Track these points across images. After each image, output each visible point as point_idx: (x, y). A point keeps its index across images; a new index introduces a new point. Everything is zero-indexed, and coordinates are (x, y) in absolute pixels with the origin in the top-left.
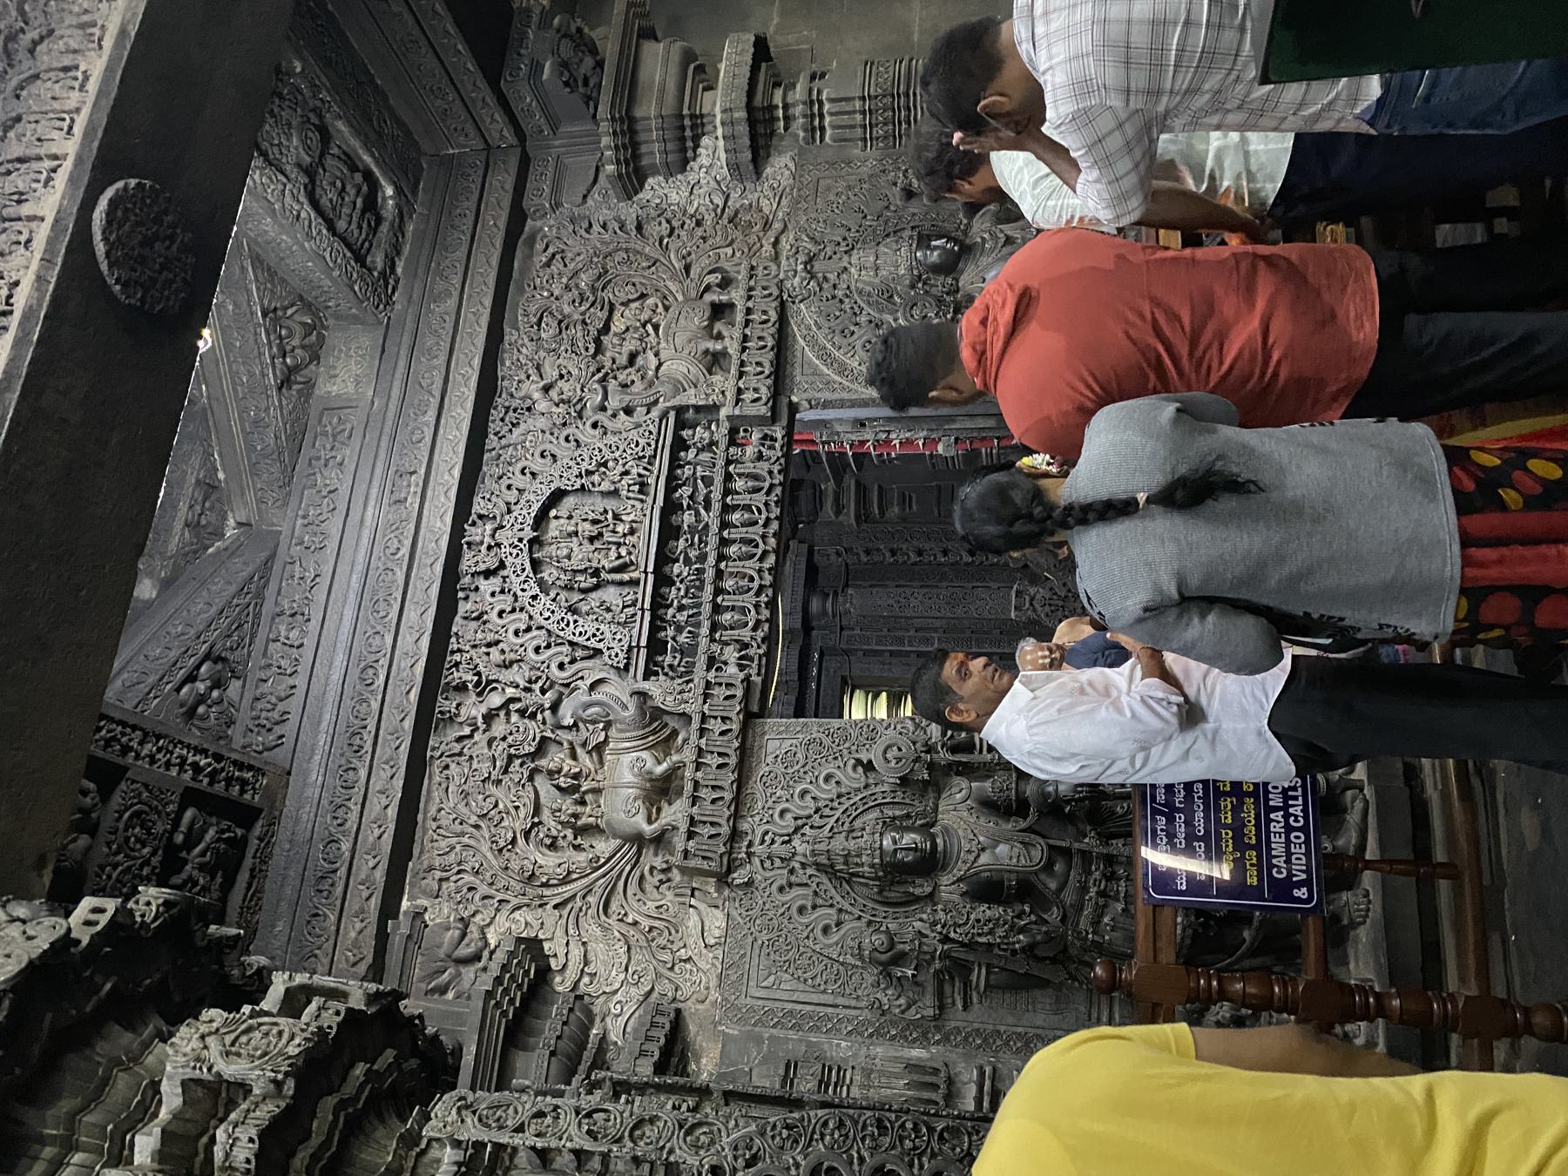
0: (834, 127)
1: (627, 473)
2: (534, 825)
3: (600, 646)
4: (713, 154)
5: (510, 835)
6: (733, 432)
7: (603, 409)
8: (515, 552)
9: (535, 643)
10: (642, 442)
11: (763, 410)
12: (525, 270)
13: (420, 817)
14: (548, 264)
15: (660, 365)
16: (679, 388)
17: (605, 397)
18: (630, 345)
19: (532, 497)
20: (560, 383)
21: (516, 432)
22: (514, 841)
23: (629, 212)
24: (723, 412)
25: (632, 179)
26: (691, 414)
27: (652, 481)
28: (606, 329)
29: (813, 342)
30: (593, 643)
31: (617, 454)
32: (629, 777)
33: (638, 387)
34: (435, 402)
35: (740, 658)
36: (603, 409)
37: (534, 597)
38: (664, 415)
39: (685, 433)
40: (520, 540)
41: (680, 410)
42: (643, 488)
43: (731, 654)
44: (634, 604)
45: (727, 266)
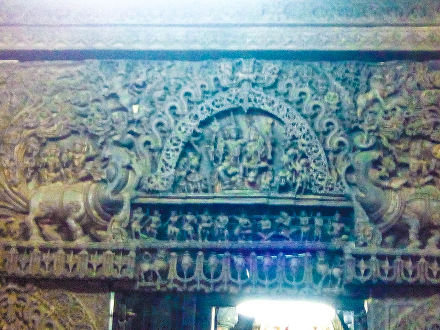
2: (39, 139)
3: (159, 170)
5: (32, 125)
8: (232, 98)
9: (165, 122)
13: (47, 62)
15: (396, 190)
19: (276, 105)
20: (381, 112)
21: (338, 84)
22: (28, 128)
27: (290, 195)
30: (161, 164)
31: (313, 165)
32: (67, 200)
33: (374, 174)
35: (154, 273)
36: (354, 149)
37: (196, 117)
38: (348, 198)
39: (337, 216)
40: (241, 101)
43: (159, 264)
44: (196, 191)
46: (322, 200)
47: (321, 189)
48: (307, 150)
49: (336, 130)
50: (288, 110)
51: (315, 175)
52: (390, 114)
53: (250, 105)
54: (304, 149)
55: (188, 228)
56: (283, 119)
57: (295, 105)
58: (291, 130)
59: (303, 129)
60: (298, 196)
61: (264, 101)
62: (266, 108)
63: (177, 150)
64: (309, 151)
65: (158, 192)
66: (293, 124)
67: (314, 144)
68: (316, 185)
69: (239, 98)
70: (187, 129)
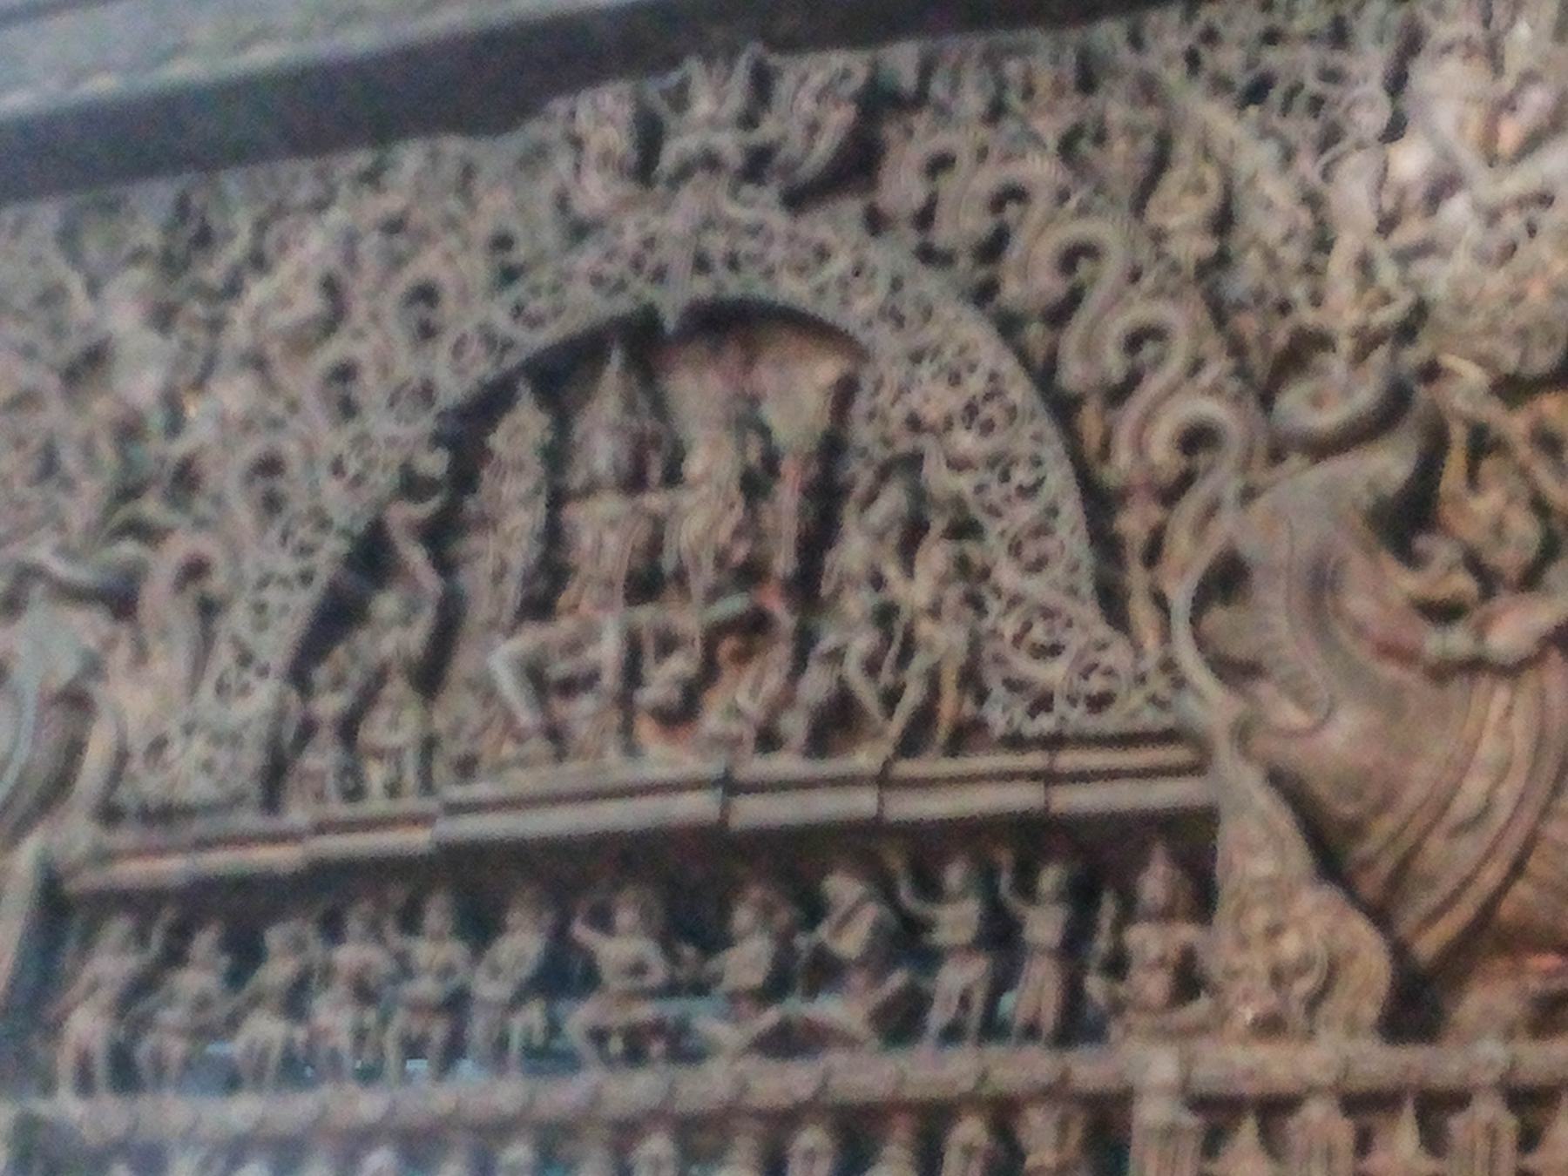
10: (1053, 673)
37: (427, 392)
46: (1049, 778)
47: (1043, 703)
48: (980, 489)
49: (1176, 364)
50: (896, 285)
51: (1010, 627)
52: (1513, 223)
53: (702, 288)
54: (964, 484)
55: (334, 1016)
56: (864, 337)
57: (964, 263)
58: (903, 390)
59: (964, 374)
60: (905, 768)
61: (777, 253)
62: (792, 290)
63: (306, 578)
64: (996, 493)
65: (188, 812)
66: (917, 358)
67: (1024, 447)
68: (1015, 685)
69: (651, 262)
70: (369, 464)
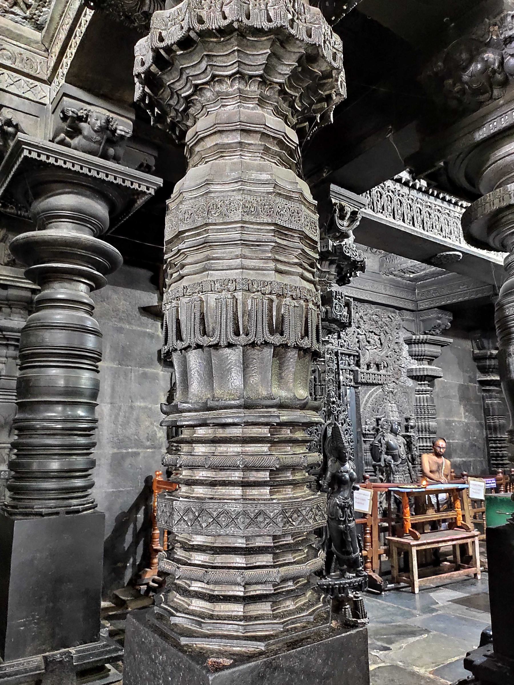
0: (420, 397)
1: (345, 341)
4: (415, 365)
6: (352, 371)
7: (358, 334)
11: (359, 380)
12: (387, 310)
14: (389, 317)
16: (364, 355)
17: (361, 335)
18: (372, 341)
23: (401, 341)
24: (357, 368)
25: (409, 342)
26: (356, 359)
28: (375, 334)
29: (373, 393)
34: (362, 287)
38: (357, 352)
39: (352, 357)
41: (358, 356)
42: (341, 346)
45: (388, 368)
